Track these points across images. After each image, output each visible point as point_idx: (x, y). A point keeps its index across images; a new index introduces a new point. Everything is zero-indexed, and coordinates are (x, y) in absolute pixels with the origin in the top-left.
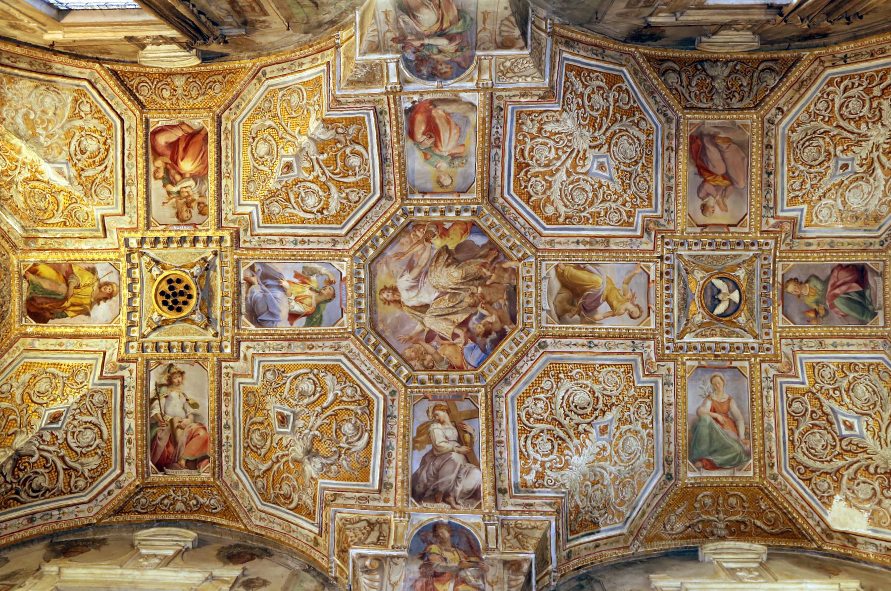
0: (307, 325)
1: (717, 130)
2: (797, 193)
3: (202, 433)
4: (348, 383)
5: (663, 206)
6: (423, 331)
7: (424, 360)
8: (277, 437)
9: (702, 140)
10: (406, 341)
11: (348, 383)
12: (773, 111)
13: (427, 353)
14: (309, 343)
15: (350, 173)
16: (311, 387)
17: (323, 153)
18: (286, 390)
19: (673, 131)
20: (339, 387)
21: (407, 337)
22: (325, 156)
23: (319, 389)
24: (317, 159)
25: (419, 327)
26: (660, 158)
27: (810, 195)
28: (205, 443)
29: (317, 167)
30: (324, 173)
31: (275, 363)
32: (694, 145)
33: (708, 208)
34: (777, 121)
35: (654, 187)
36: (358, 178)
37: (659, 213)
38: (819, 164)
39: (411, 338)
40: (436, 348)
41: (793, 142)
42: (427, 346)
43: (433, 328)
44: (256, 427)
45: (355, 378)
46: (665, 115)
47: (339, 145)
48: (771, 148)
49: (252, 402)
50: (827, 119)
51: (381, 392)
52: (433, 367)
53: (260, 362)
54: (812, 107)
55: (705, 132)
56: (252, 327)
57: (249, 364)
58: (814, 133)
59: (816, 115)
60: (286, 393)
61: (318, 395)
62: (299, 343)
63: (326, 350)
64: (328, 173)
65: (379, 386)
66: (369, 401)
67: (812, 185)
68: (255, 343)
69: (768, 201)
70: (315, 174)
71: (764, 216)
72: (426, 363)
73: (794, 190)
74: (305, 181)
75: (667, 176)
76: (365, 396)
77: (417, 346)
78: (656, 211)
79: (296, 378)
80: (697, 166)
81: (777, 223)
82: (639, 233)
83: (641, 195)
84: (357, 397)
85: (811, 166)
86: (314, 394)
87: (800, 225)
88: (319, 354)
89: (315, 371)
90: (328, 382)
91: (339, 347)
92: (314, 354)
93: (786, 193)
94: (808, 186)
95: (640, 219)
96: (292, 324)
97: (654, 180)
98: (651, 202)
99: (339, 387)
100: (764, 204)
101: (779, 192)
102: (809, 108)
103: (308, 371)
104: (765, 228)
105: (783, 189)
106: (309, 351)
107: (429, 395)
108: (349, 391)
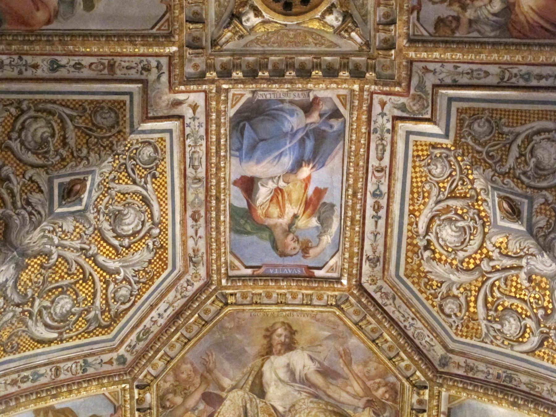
0: (234, 210)
3: (41, 15)
4: (136, 287)
6: (222, 389)
7: (175, 393)
8: (42, 179)
10: (205, 364)
11: (136, 287)
13: (186, 397)
14: (203, 213)
15: (491, 313)
16: (128, 229)
17: (530, 280)
18: (123, 187)
20: (130, 273)
21: (211, 366)
22: (526, 284)
23: (126, 242)
24: (520, 267)
25: (227, 382)
28: (22, 21)
29: (507, 262)
30: (495, 270)
31: (168, 159)
36: (483, 323)
39: (210, 371)
40: (193, 410)
42: (197, 396)
43: (227, 403)
44: (56, 128)
45: (145, 296)
47: (541, 312)
49: (99, 120)
51: (122, 342)
52: (164, 407)
53: (170, 131)
56: (232, 112)
57: (165, 112)
60: (118, 187)
61: (116, 242)
62: (202, 196)
63: (191, 243)
64: (497, 276)
65: (133, 337)
66: (108, 327)
68: (203, 119)
70: (495, 254)
72: (170, 396)
74: (485, 234)
76: (117, 317)
77: (197, 380)
79: (145, 200)
84: (114, 306)
86: (118, 236)
88: (184, 233)
89: (156, 231)
90: (137, 256)
91: (195, 264)
92: (183, 222)
96: (235, 183)
99: (130, 273)
103: (156, 220)
106: (189, 212)
107: (119, 412)
108: (124, 292)
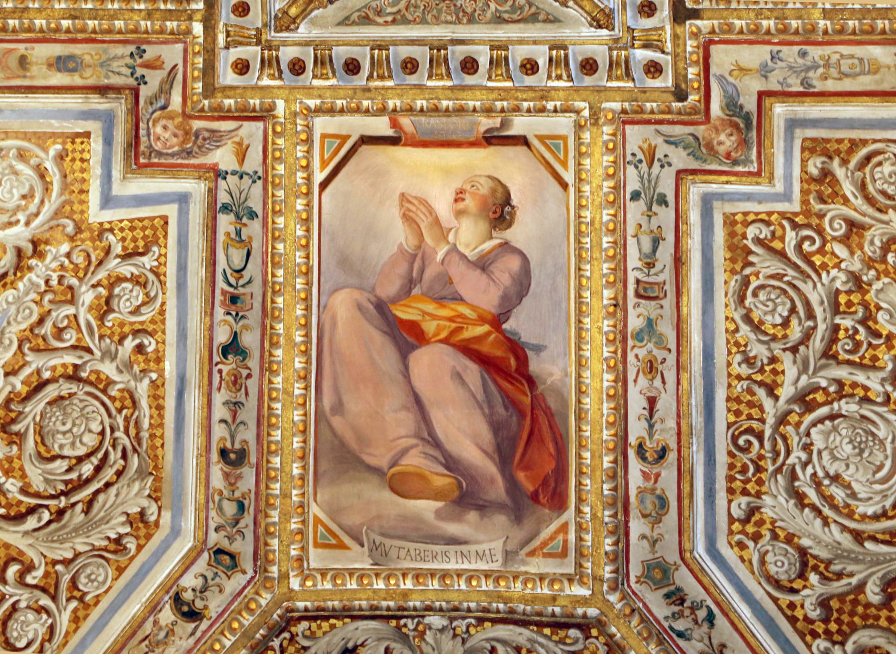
1: (453, 529)
2: (127, 270)
5: (679, 218)
9: (512, 485)
12: (214, 604)
19: (637, 527)
26: (697, 419)
27: (79, 259)
32: (549, 467)
33: (484, 207)
34: (201, 565)
35: (720, 298)
37: (695, 191)
38: (42, 385)
41: (142, 473)
46: (676, 597)
48: (224, 453)
50: (12, 571)
54: (64, 620)
55: (501, 520)
58: (60, 513)
59: (49, 588)
67: (72, 302)
69: (239, 239)
71: (255, 178)
73: (138, 281)
75: (661, 343)
78: (707, 202)
80: (531, 382)
81: (202, 150)
82: (780, 110)
83: (776, 266)
85: (74, 376)
87: (108, 141)
93: (171, 270)
94: (87, 297)
95: (779, 171)
97: (720, 326)
98: (732, 234)
100: (254, 228)
101: (197, 273)
102: (76, 620)
104: (252, 131)
105: (181, 286)
